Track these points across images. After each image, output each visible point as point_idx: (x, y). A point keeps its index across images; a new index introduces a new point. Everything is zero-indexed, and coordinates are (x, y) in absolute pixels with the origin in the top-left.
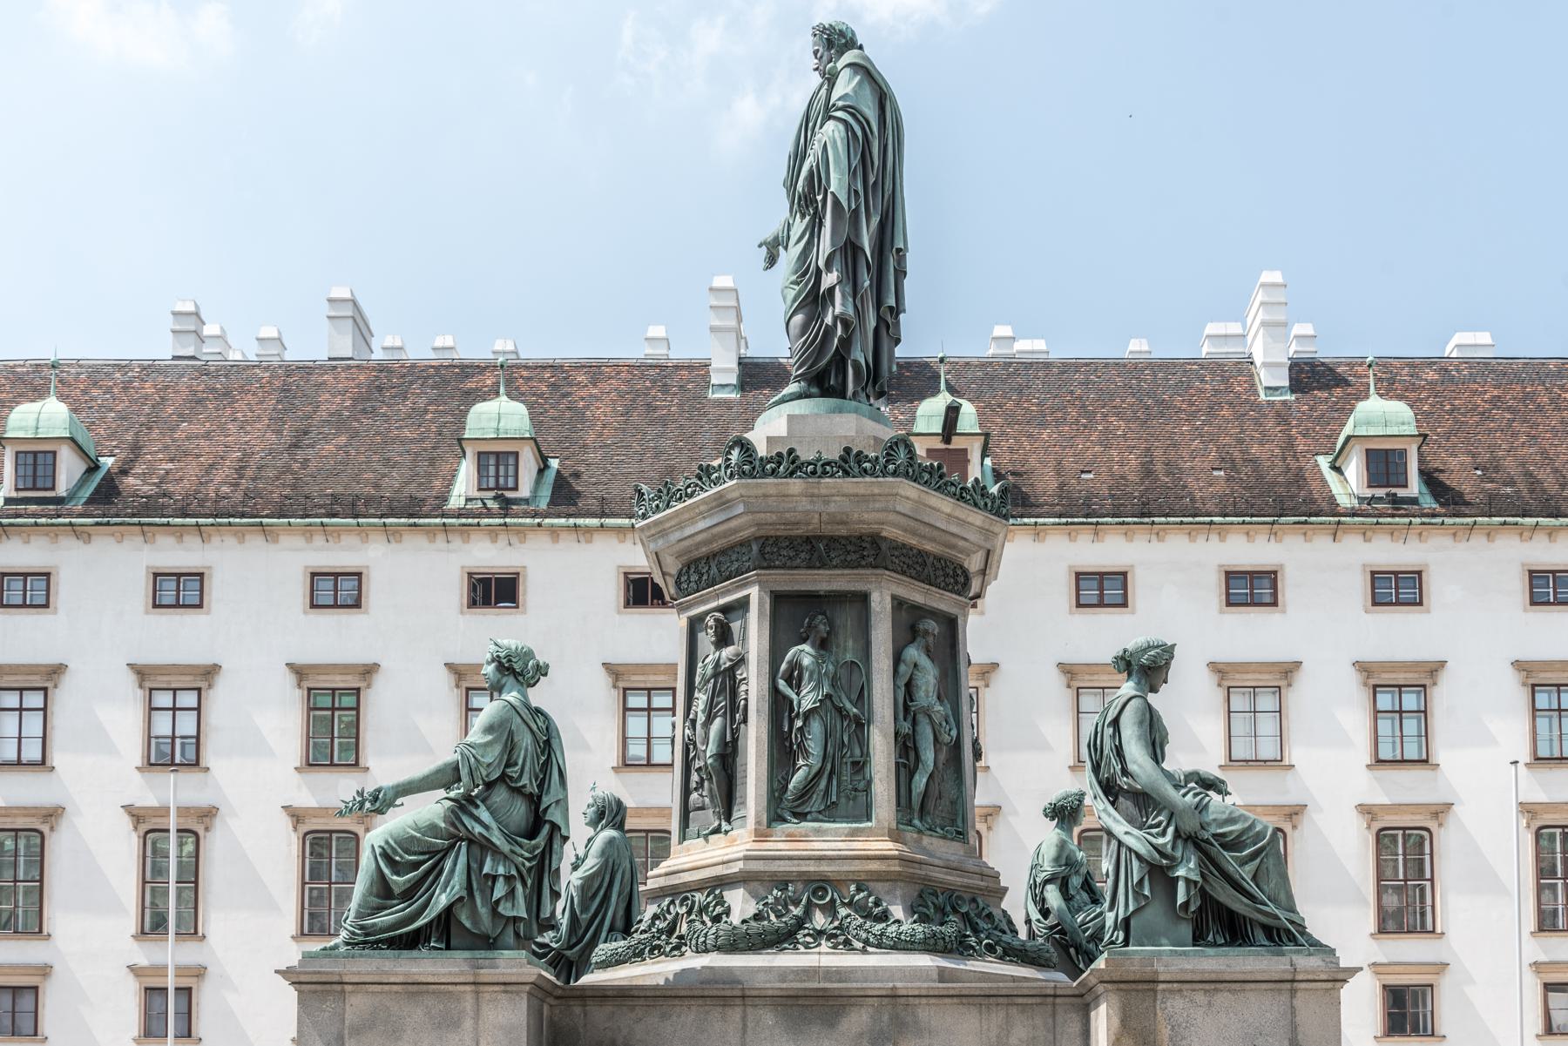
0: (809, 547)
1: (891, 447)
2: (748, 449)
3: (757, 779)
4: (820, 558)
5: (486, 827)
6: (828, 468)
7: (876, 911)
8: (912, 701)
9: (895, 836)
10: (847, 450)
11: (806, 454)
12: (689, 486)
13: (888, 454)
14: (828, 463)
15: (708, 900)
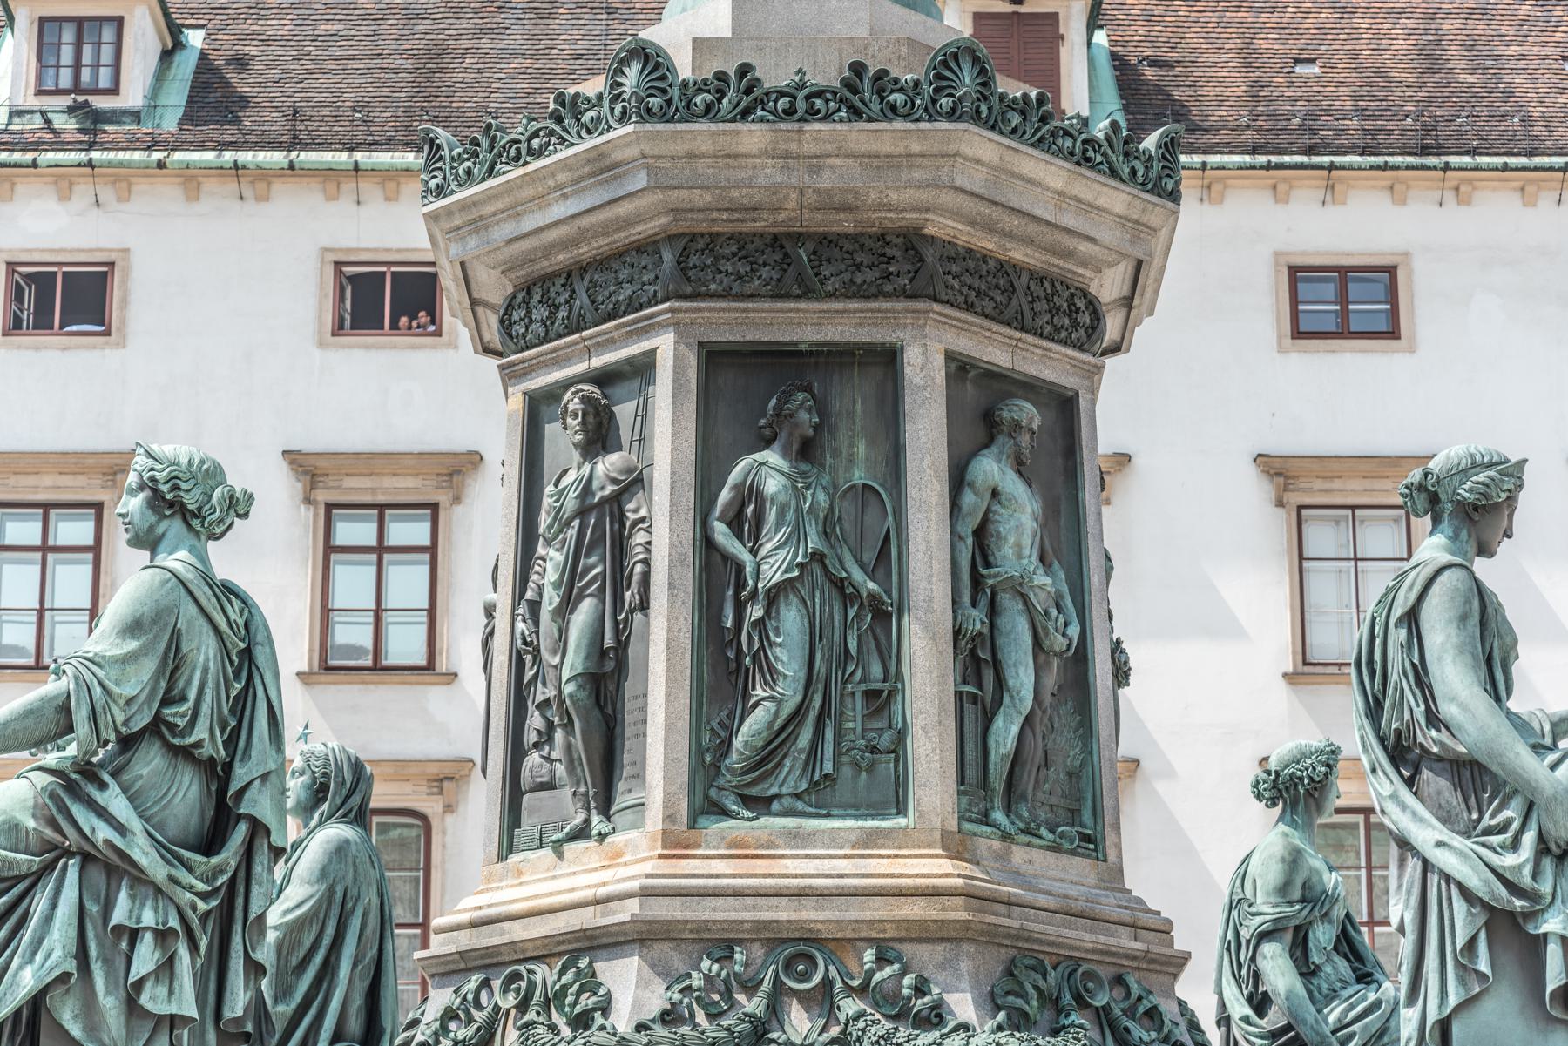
0: (778, 256)
1: (944, 63)
2: (657, 66)
3: (669, 728)
4: (800, 279)
5: (121, 829)
6: (819, 103)
7: (919, 1004)
8: (988, 565)
9: (957, 847)
10: (858, 68)
11: (774, 75)
12: (535, 134)
13: (939, 77)
14: (819, 94)
15: (564, 980)
